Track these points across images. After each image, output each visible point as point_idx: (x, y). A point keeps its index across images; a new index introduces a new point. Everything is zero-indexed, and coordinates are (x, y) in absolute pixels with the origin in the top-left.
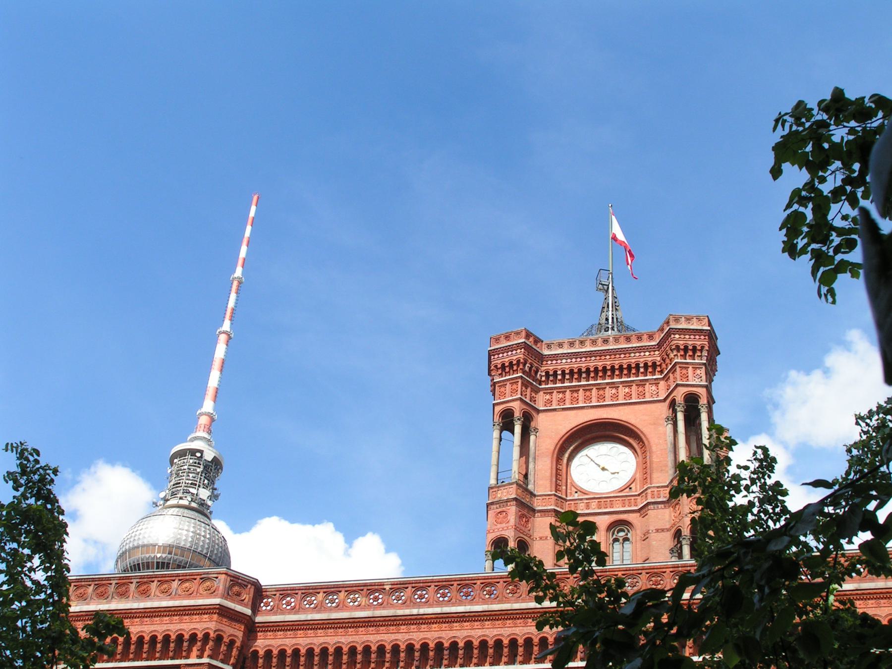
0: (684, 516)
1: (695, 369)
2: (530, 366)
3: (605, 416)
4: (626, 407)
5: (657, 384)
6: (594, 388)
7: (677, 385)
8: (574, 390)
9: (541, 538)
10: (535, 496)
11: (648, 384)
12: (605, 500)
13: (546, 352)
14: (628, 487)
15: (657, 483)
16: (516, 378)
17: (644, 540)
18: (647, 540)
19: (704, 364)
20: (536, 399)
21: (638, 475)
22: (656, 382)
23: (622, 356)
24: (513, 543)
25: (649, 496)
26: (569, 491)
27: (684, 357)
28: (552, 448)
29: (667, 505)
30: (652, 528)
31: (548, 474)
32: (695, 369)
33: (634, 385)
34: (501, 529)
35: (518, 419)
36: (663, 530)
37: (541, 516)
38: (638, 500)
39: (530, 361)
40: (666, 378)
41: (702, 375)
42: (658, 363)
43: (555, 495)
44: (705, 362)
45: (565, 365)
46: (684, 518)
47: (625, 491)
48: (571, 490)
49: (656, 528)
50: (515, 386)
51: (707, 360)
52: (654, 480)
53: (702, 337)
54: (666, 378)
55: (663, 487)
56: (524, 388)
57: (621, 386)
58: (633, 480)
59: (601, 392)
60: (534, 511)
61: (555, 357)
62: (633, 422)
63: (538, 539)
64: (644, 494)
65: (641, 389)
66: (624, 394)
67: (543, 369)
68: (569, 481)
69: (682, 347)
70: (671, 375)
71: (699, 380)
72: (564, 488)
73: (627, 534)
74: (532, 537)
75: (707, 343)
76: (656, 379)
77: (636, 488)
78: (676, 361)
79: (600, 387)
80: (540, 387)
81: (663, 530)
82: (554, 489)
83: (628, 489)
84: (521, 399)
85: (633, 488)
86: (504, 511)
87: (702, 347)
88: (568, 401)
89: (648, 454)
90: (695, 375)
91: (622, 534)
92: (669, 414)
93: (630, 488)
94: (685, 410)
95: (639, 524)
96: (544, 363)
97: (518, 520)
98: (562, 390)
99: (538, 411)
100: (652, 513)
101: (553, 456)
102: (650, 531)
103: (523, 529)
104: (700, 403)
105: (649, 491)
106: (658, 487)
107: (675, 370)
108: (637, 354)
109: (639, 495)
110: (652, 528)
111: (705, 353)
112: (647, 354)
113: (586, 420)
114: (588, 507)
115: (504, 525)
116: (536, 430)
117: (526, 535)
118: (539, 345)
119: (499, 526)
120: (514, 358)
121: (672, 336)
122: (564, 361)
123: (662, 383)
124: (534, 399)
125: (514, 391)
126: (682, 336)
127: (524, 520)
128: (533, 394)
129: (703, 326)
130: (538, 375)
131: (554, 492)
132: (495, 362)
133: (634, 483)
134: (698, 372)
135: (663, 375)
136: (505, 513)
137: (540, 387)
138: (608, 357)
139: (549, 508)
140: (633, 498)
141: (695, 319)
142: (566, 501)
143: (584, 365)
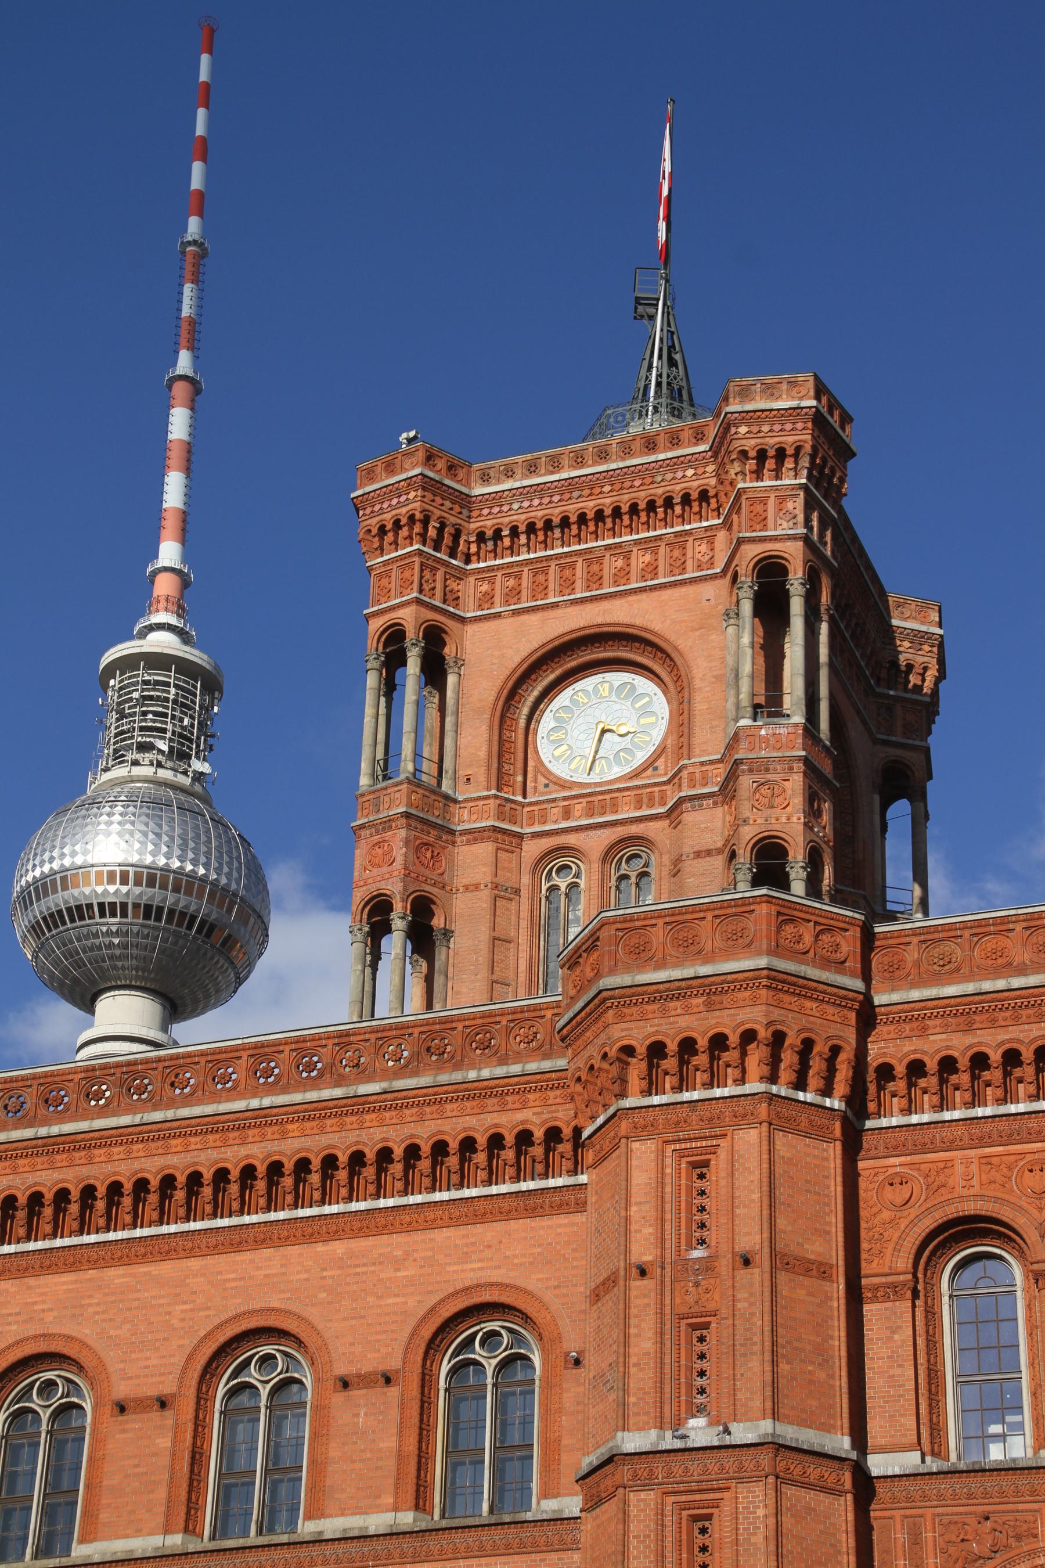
1: (782, 500)
3: (600, 620)
4: (644, 596)
5: (711, 541)
7: (740, 542)
8: (539, 567)
9: (467, 888)
11: (691, 539)
12: (600, 797)
13: (479, 490)
14: (650, 764)
15: (700, 756)
19: (802, 486)
20: (460, 594)
22: (709, 536)
26: (530, 784)
27: (758, 475)
28: (492, 698)
29: (720, 798)
30: (687, 849)
31: (483, 754)
32: (782, 500)
34: (378, 878)
36: (709, 853)
37: (469, 843)
38: (669, 793)
39: (438, 513)
40: (727, 525)
41: (797, 512)
42: (712, 493)
43: (496, 797)
44: (804, 481)
45: (518, 514)
47: (644, 775)
48: (536, 781)
50: (407, 574)
51: (809, 477)
52: (697, 751)
53: (800, 426)
54: (727, 525)
55: (712, 762)
56: (427, 574)
57: (635, 549)
58: (660, 752)
59: (595, 568)
60: (452, 832)
62: (656, 626)
64: (676, 780)
65: (676, 553)
66: (641, 566)
67: (473, 526)
68: (531, 763)
69: (752, 454)
70: (735, 517)
71: (791, 524)
72: (520, 778)
73: (646, 865)
74: (448, 888)
76: (708, 529)
78: (740, 486)
79: (591, 558)
80: (469, 567)
81: (709, 853)
82: (494, 783)
83: (649, 772)
85: (661, 770)
86: (385, 841)
87: (798, 449)
89: (686, 694)
91: (638, 864)
92: (730, 603)
93: (656, 769)
94: (756, 593)
95: (668, 842)
96: (475, 514)
97: (412, 856)
98: (513, 572)
99: (462, 620)
100: (690, 817)
101: (493, 715)
102: (684, 857)
103: (427, 872)
104: (790, 577)
105: (685, 774)
106: (702, 764)
107: (740, 508)
108: (669, 476)
109: (669, 782)
110: (687, 849)
111: (805, 462)
112: (690, 472)
113: (567, 629)
115: (385, 869)
116: (460, 663)
118: (461, 474)
119: (376, 871)
121: (733, 430)
122: (515, 506)
123: (722, 535)
124: (454, 596)
125: (405, 585)
126: (755, 429)
127: (429, 855)
129: (801, 398)
130: (462, 542)
131: (493, 792)
132: (366, 523)
134: (790, 505)
135: (722, 517)
138: (607, 488)
139: (484, 824)
140: (657, 789)
141: (784, 386)
142: (523, 805)
143: (557, 511)
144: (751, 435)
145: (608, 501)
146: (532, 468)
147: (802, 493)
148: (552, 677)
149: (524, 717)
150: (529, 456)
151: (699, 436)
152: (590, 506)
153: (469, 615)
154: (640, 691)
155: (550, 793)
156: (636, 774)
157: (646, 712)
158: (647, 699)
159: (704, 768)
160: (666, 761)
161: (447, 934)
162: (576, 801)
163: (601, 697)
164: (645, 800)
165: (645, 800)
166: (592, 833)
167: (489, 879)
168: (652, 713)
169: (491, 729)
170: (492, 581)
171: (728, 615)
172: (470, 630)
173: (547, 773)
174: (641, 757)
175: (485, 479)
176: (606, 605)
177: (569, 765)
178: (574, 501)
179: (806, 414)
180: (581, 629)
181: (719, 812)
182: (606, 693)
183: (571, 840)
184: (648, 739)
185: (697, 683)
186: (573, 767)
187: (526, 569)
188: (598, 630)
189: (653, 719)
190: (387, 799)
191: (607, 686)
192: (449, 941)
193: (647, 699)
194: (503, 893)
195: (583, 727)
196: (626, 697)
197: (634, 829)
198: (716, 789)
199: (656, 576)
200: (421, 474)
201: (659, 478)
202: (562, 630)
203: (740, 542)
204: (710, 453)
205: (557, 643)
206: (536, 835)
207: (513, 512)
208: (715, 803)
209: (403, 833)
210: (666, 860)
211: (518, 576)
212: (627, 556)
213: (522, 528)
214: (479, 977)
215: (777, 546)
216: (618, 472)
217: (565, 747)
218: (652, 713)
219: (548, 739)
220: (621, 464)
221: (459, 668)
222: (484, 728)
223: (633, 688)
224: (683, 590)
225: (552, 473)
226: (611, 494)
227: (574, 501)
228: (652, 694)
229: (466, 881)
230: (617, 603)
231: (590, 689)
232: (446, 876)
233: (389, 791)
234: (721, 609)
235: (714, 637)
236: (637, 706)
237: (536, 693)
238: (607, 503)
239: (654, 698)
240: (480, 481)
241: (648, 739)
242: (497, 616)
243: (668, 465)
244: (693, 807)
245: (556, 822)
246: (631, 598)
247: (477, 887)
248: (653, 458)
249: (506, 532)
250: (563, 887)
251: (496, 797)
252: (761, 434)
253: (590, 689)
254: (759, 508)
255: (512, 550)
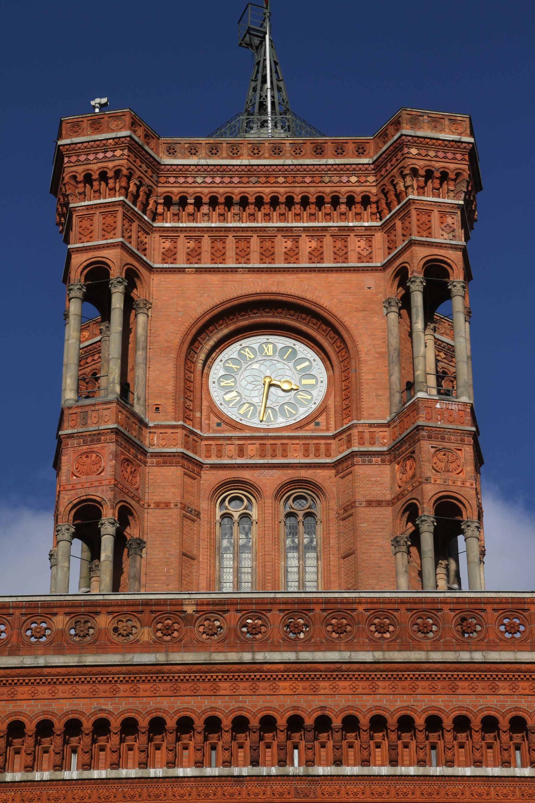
0: (423, 480)
2: (138, 183)
3: (274, 289)
4: (313, 275)
5: (369, 239)
6: (255, 236)
9: (158, 505)
10: (146, 426)
11: (352, 235)
13: (167, 160)
15: (368, 419)
16: (113, 204)
17: (343, 519)
18: (350, 518)
20: (147, 246)
21: (331, 402)
23: (308, 180)
24: (111, 511)
25: (355, 439)
28: (177, 341)
29: (388, 457)
31: (170, 388)
32: (443, 214)
33: (328, 235)
35: (119, 282)
36: (379, 503)
37: (158, 465)
38: (333, 447)
42: (373, 199)
43: (183, 427)
46: (424, 486)
47: (306, 428)
49: (368, 498)
50: (110, 220)
52: (365, 414)
55: (380, 425)
57: (303, 235)
58: (323, 409)
59: (268, 244)
60: (145, 453)
61: (183, 170)
62: (325, 302)
63: (152, 506)
64: (344, 436)
67: (160, 190)
69: (422, 172)
71: (451, 236)
74: (141, 503)
75: (466, 167)
77: (328, 423)
80: (155, 225)
81: (379, 503)
83: (312, 426)
84: (123, 246)
85: (323, 425)
86: (93, 452)
88: (206, 255)
90: (443, 226)
93: (317, 424)
95: (334, 489)
96: (162, 180)
99: (150, 269)
102: (357, 504)
105: (355, 432)
106: (371, 425)
109: (334, 437)
112: (354, 179)
114: (241, 452)
116: (148, 305)
117: (132, 498)
119: (83, 478)
120: (110, 165)
121: (406, 150)
124: (143, 247)
128: (143, 238)
131: (181, 423)
133: (324, 414)
135: (383, 222)
136: (94, 455)
137: (155, 225)
138: (281, 180)
139: (174, 450)
140: (323, 442)
142: (202, 438)
143: (237, 191)
144: (420, 157)
145: (282, 190)
146: (214, 151)
147: (459, 212)
148: (226, 331)
149: (201, 362)
150: (211, 140)
151: (361, 151)
152: (267, 191)
153: (156, 266)
154: (300, 355)
155: (223, 431)
156: (301, 425)
157: (306, 374)
158: (307, 363)
159: (372, 430)
160: (327, 419)
161: (141, 544)
162: (249, 442)
163: (266, 355)
164: (323, 448)
165: (312, 449)
166: (265, 472)
167: (178, 499)
168: (313, 377)
169: (177, 367)
170: (174, 240)
171: (389, 303)
172: (156, 279)
173: (219, 414)
174: (303, 413)
175: (171, 151)
176: (279, 277)
177: (239, 409)
178: (251, 185)
179: (465, 148)
180: (257, 294)
181: (387, 469)
182: (270, 353)
183: (246, 475)
184: (309, 397)
185: (363, 356)
186: (242, 411)
187: (206, 235)
188: (272, 297)
189: (313, 382)
190: (94, 414)
191: (271, 346)
192: (141, 550)
193: (307, 363)
194: (189, 514)
195: (250, 379)
196: (289, 359)
197: (304, 474)
198: (385, 449)
199: (321, 260)
200: (130, 136)
201: (327, 179)
202: (240, 293)
203: (412, 243)
204: (372, 166)
205: (236, 302)
206: (214, 467)
207: (196, 185)
208: (383, 461)
209: (113, 447)
210: (333, 504)
211: (198, 240)
212: (296, 239)
213: (206, 200)
214: (170, 587)
215: (442, 252)
216: (292, 167)
217: (234, 394)
218: (313, 377)
219: (219, 384)
220: (295, 162)
221: (148, 310)
222: (171, 366)
223: (294, 351)
224: (347, 276)
225: (232, 158)
226: (284, 185)
227: (251, 185)
228: (312, 359)
229: (156, 499)
230: (289, 278)
231: (256, 346)
232: (140, 491)
233: (97, 408)
234: (381, 297)
235: (376, 319)
236: (299, 368)
237: (212, 343)
238: (282, 191)
239: (314, 364)
240: (167, 153)
241: (309, 397)
242: (182, 270)
243: (335, 170)
244: (364, 461)
245: (231, 457)
246: (302, 276)
247: (167, 505)
248: (323, 161)
249: (191, 201)
250: (236, 516)
251: (183, 427)
252: (429, 158)
253: (256, 346)
254: (424, 218)
255: (192, 217)
